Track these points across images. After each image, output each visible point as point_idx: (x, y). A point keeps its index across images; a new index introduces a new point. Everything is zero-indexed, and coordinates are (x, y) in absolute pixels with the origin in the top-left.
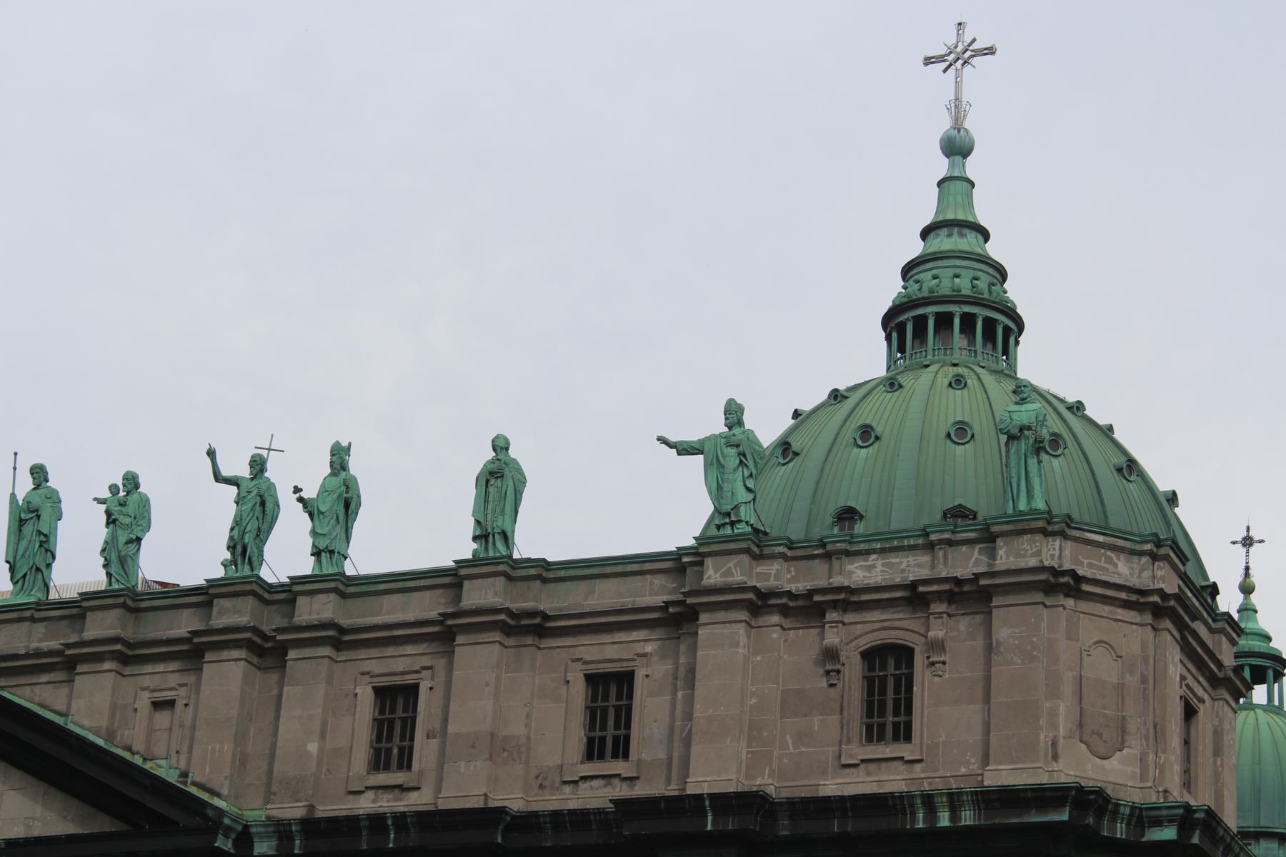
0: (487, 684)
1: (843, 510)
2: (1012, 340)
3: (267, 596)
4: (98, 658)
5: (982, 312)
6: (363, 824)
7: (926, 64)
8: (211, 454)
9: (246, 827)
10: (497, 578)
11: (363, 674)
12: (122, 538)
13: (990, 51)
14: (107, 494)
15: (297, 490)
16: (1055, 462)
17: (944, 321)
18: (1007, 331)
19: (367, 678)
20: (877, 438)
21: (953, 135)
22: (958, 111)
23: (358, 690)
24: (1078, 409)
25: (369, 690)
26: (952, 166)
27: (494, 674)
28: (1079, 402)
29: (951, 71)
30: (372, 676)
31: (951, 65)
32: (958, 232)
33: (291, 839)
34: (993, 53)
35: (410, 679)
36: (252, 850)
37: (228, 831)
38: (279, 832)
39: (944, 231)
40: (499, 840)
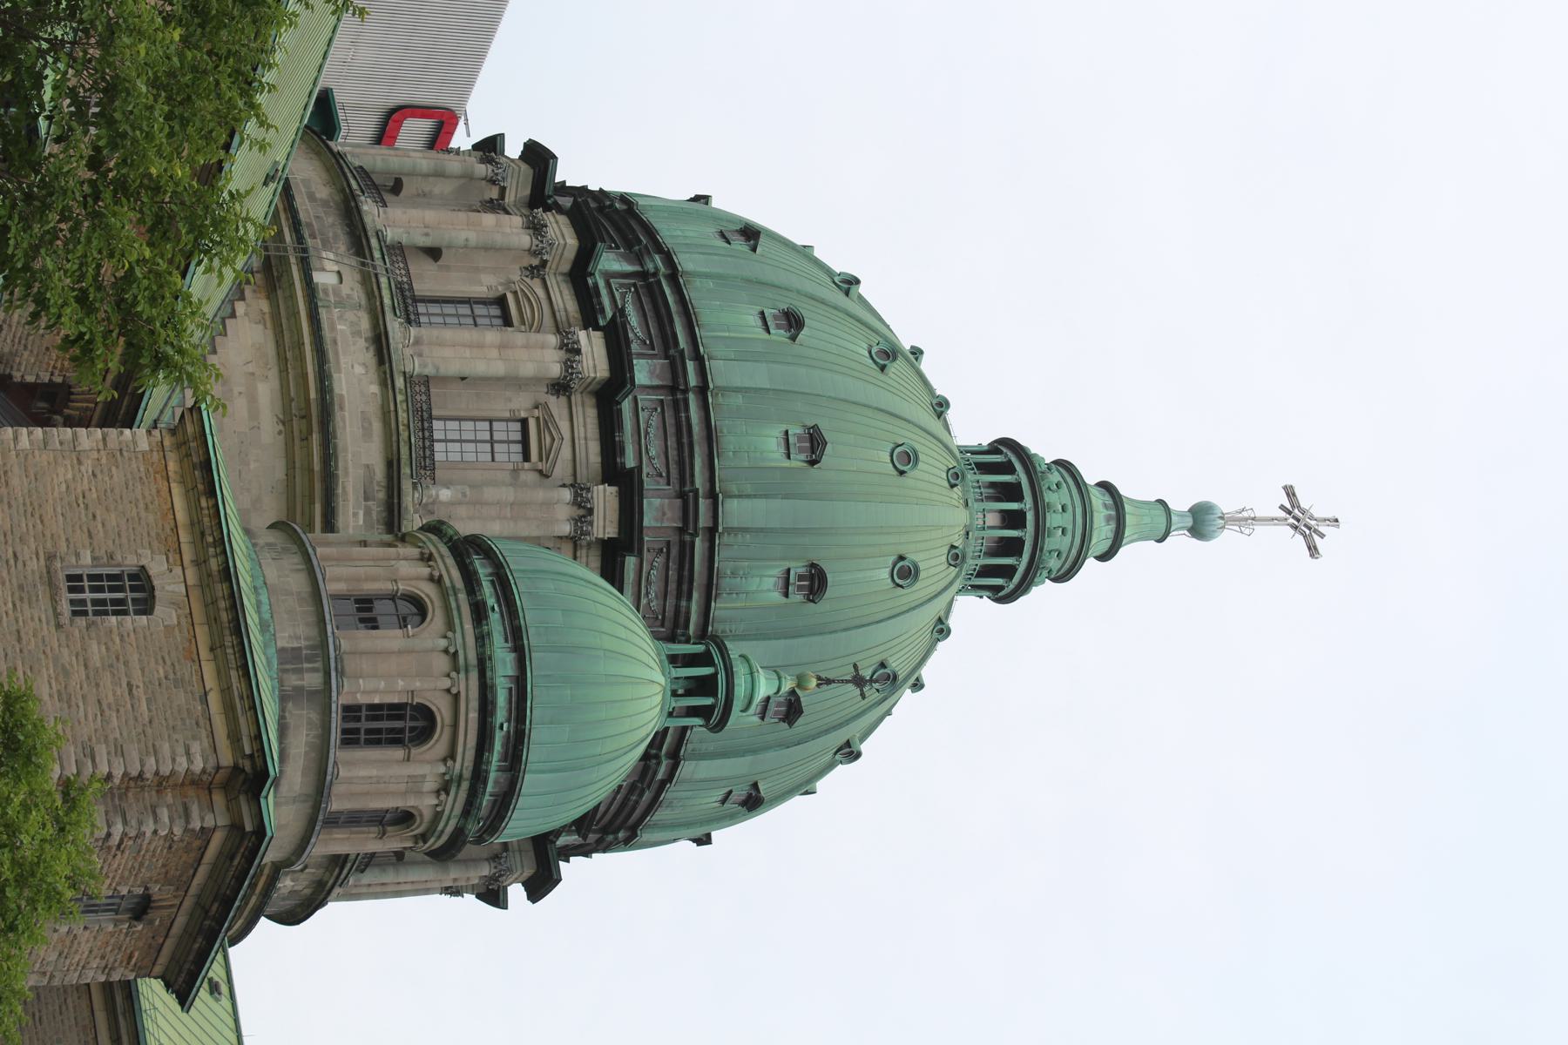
1: (799, 317)
2: (999, 581)
5: (1028, 535)
7: (1285, 488)
13: (1313, 550)
16: (885, 574)
17: (1012, 492)
18: (1008, 572)
20: (883, 368)
21: (1215, 511)
22: (1245, 521)
24: (941, 631)
26: (1181, 515)
28: (949, 632)
29: (1283, 514)
31: (1289, 513)
32: (1110, 515)
34: (1312, 556)
39: (1109, 501)
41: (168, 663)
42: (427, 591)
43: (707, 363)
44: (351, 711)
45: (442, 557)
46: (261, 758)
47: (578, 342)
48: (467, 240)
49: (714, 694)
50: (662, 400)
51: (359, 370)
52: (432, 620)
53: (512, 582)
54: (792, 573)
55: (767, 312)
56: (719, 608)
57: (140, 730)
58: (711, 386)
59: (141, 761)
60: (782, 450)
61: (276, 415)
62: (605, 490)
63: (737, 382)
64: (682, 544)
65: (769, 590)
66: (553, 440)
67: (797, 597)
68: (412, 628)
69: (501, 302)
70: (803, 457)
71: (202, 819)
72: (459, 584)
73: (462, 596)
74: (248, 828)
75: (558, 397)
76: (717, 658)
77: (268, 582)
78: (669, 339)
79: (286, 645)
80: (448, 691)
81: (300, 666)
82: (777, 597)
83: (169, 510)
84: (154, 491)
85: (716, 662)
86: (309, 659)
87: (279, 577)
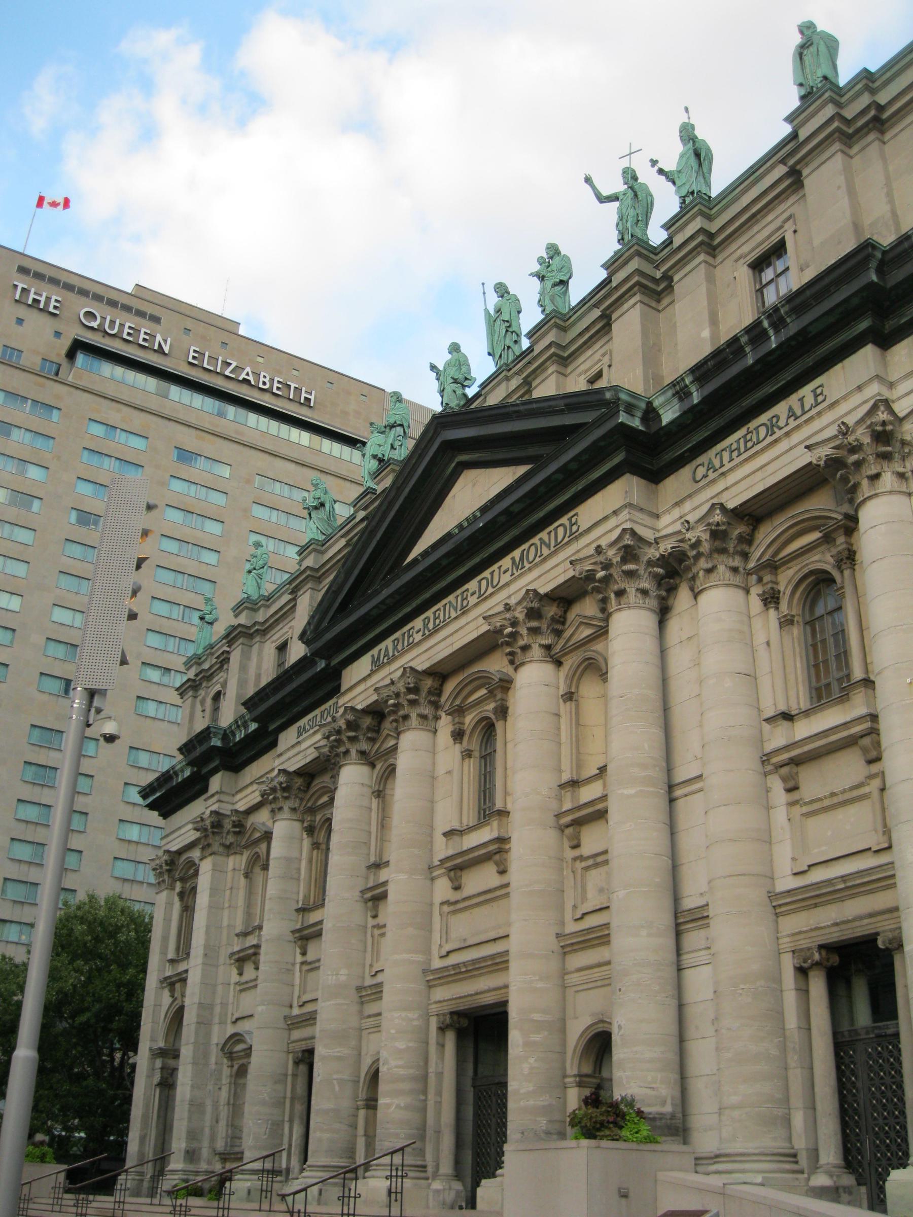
0: (839, 187)
3: (652, 256)
4: (542, 367)
6: (744, 340)
8: (588, 180)
9: (649, 404)
10: (826, 108)
11: (736, 261)
12: (549, 284)
14: (536, 267)
15: (654, 163)
19: (742, 261)
23: (735, 274)
25: (745, 268)
27: (843, 177)
30: (746, 256)
33: (690, 394)
35: (775, 239)
36: (660, 421)
37: (630, 409)
38: (677, 393)
40: (874, 278)
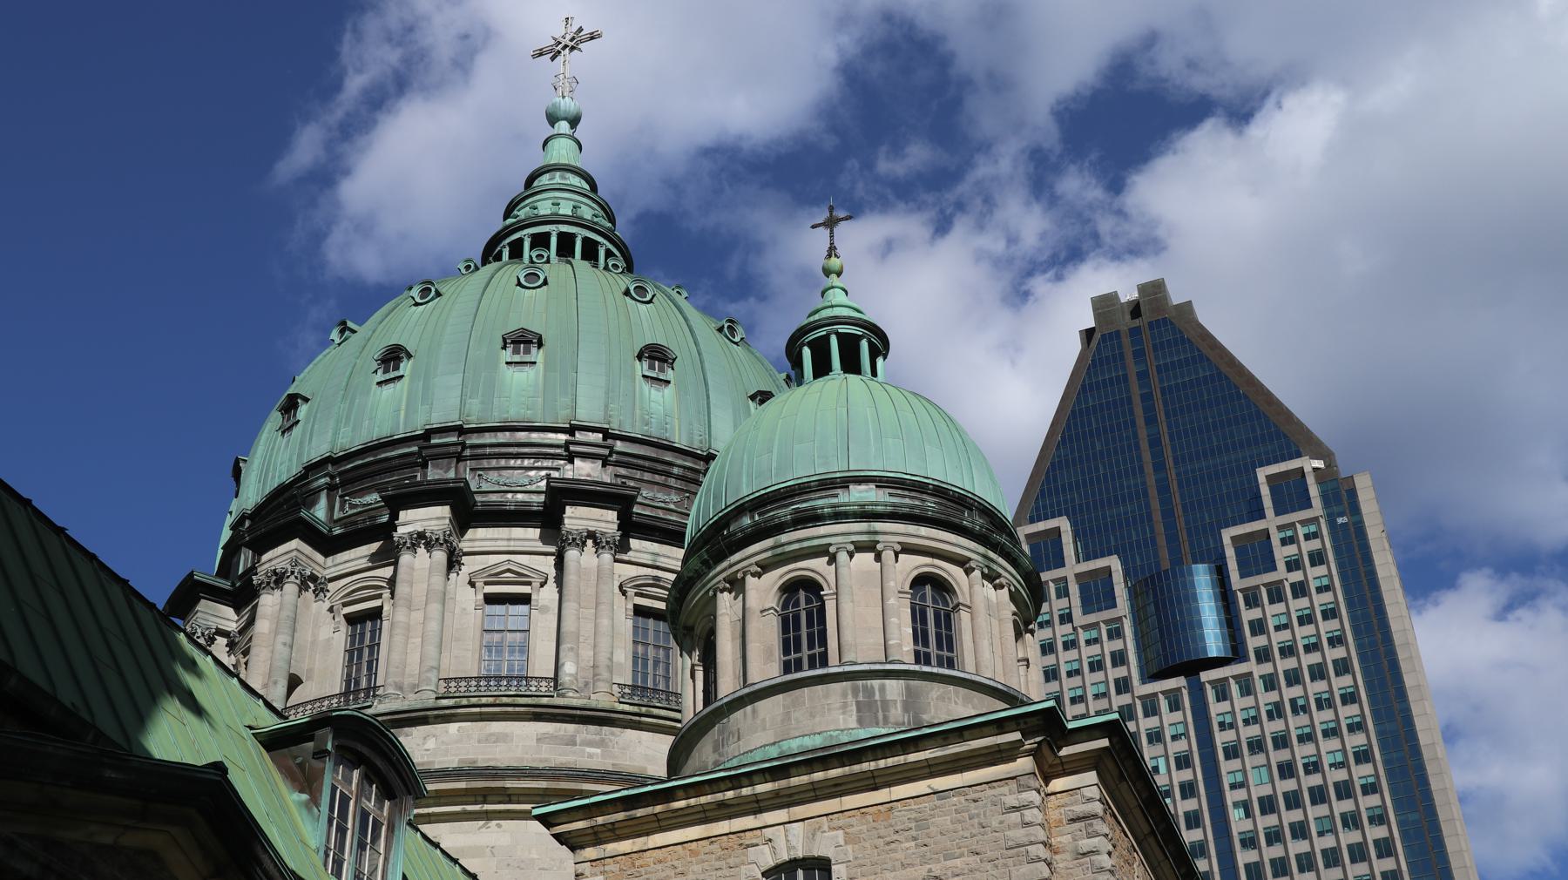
1: (387, 350)
5: (582, 233)
16: (643, 307)
17: (541, 241)
34: (599, 36)
41: (896, 837)
42: (776, 577)
43: (435, 426)
44: (919, 658)
45: (731, 566)
46: (1028, 720)
47: (410, 534)
48: (285, 644)
49: (858, 338)
50: (470, 469)
51: (431, 744)
52: (813, 571)
53: (763, 492)
54: (647, 374)
55: (380, 377)
56: (681, 441)
57: (989, 866)
58: (459, 423)
59: (1033, 861)
60: (527, 368)
61: (479, 829)
62: (570, 518)
63: (455, 401)
64: (618, 464)
65: (663, 396)
66: (509, 570)
67: (669, 374)
68: (823, 590)
69: (351, 620)
70: (534, 350)
71: (1090, 800)
72: (769, 542)
73: (784, 538)
74: (1105, 743)
75: (463, 564)
76: (822, 332)
77: (772, 741)
78: (407, 463)
79: (854, 717)
80: (896, 555)
81: (879, 703)
82: (669, 391)
83: (684, 848)
84: (659, 867)
85: (824, 333)
86: (869, 692)
87: (764, 729)
